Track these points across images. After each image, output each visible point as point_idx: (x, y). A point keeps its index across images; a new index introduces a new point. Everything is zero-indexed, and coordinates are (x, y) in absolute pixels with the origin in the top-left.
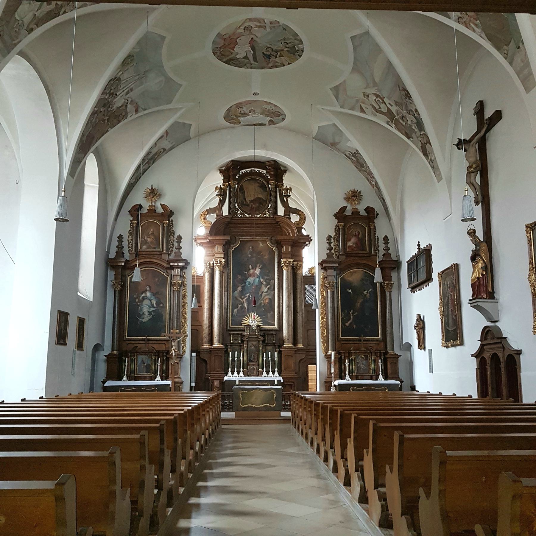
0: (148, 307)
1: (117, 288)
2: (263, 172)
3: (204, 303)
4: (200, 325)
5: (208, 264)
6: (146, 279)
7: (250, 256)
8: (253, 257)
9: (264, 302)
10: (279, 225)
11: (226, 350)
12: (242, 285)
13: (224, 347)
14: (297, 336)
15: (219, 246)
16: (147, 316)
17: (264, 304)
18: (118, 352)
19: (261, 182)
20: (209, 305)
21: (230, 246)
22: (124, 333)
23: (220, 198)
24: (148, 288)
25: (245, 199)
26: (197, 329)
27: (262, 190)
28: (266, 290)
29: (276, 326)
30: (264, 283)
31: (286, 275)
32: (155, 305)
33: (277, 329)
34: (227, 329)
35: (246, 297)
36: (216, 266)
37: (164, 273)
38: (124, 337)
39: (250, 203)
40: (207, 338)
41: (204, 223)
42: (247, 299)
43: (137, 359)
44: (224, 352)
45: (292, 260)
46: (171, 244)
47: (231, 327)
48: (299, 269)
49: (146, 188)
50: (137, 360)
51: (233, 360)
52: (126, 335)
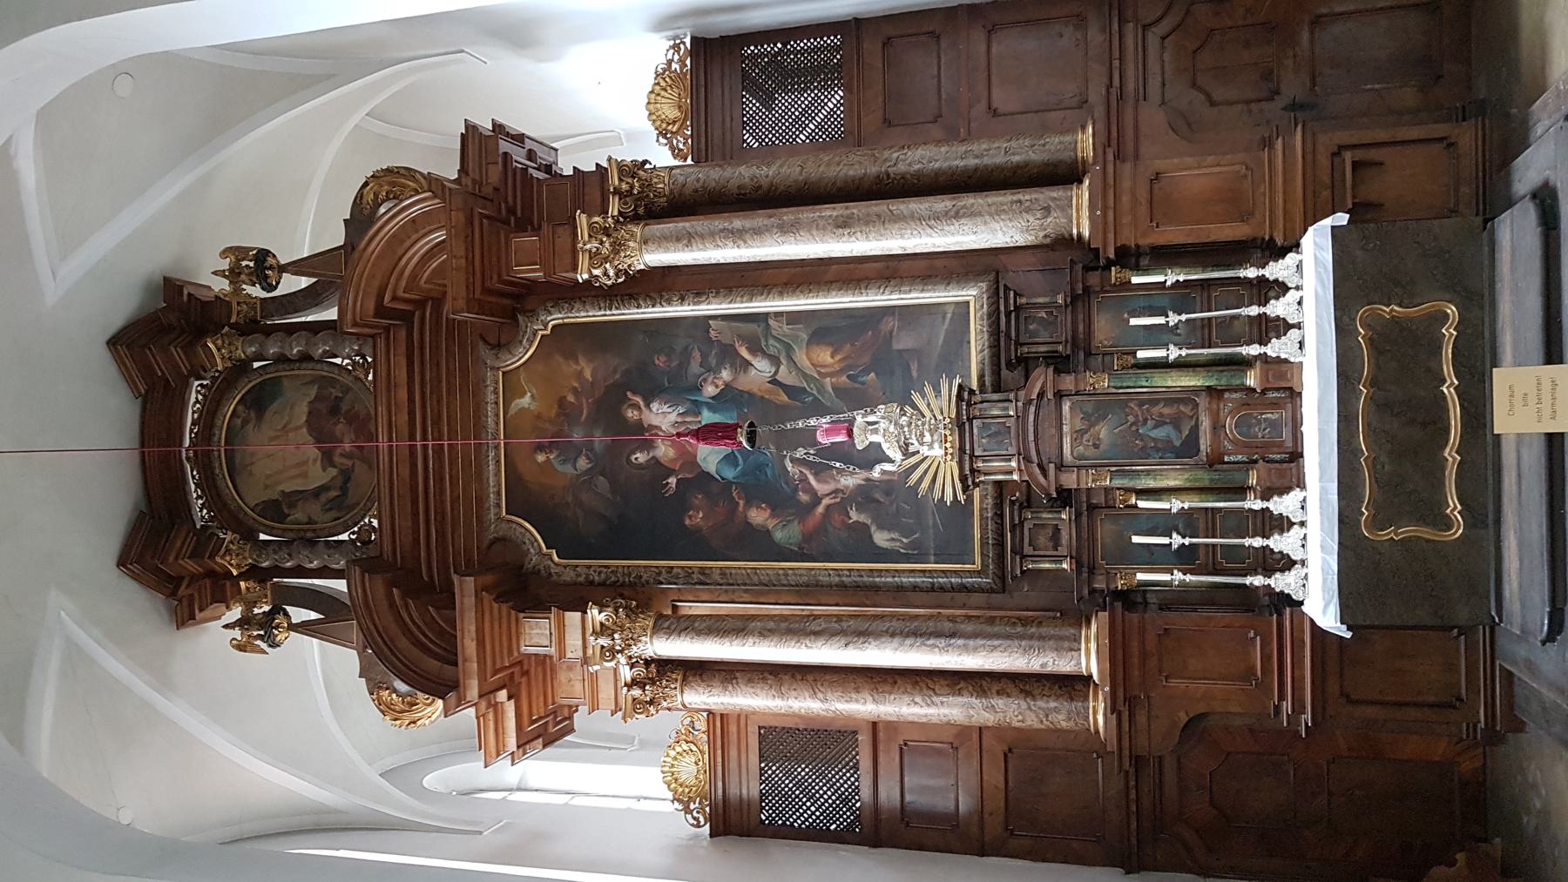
2: (197, 401)
3: (850, 718)
4: (975, 736)
5: (637, 692)
7: (583, 463)
8: (589, 446)
9: (831, 375)
10: (421, 304)
11: (1118, 605)
12: (741, 503)
13: (1104, 616)
14: (1026, 164)
15: (522, 644)
17: (841, 371)
19: (240, 408)
20: (857, 690)
23: (305, 628)
25: (317, 493)
26: (999, 750)
27: (275, 406)
28: (762, 367)
29: (971, 294)
30: (726, 375)
31: (667, 250)
33: (984, 285)
34: (992, 591)
35: (804, 480)
39: (334, 467)
40: (1053, 704)
41: (430, 709)
42: (816, 475)
44: (1134, 617)
45: (582, 220)
47: (978, 566)
48: (647, 185)
51: (1186, 558)
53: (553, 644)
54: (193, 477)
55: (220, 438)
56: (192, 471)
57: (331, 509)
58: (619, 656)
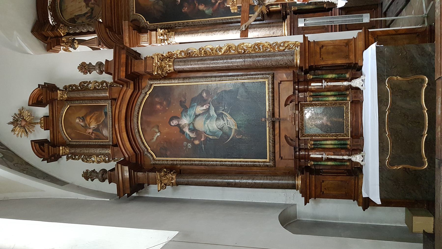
0: (209, 121)
1: (172, 178)
6: (158, 127)
12: (197, 4)
16: (226, 122)
18: (298, 176)
21: (143, 28)
22: (260, 166)
24: (174, 123)
32: (205, 107)
36: (169, 42)
37: (146, 93)
38: (267, 166)
39: (89, 7)
43: (312, 136)
46: (102, 86)
49: (13, 133)
50: (315, 136)
52: (264, 162)
53: (148, 41)
54: (50, 14)
55: (58, 2)
56: (50, 12)
57: (88, 19)
58: (166, 41)
